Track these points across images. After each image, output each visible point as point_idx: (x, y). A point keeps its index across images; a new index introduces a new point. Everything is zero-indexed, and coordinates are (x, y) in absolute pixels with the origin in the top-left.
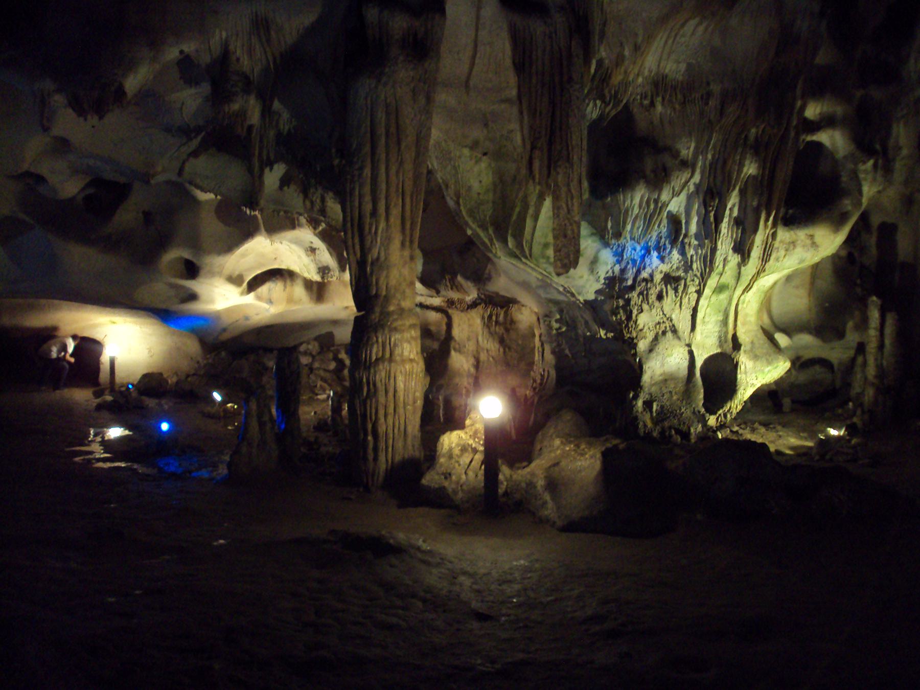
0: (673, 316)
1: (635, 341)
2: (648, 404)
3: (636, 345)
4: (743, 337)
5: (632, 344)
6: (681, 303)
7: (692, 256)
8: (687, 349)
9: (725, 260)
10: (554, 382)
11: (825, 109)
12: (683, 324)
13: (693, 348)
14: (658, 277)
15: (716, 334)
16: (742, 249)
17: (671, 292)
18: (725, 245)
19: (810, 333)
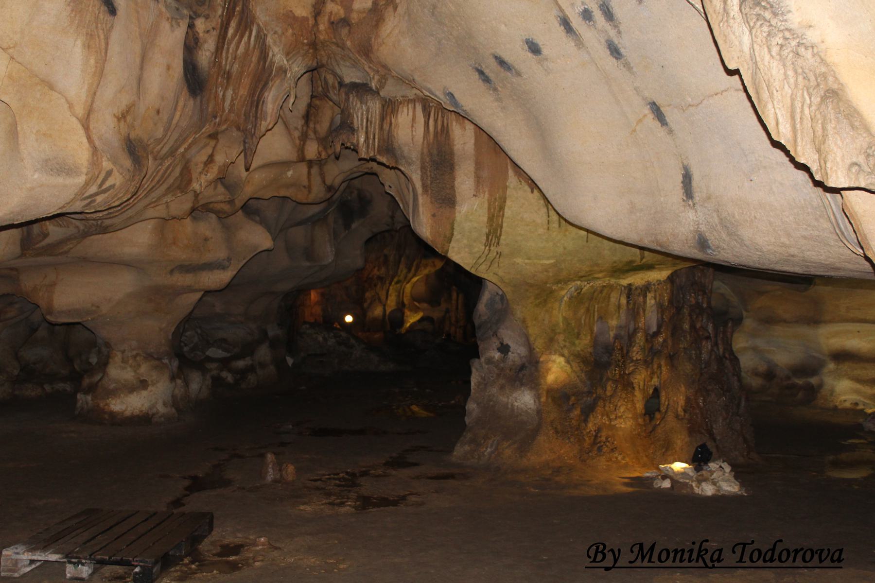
4: (406, 301)
18: (402, 266)
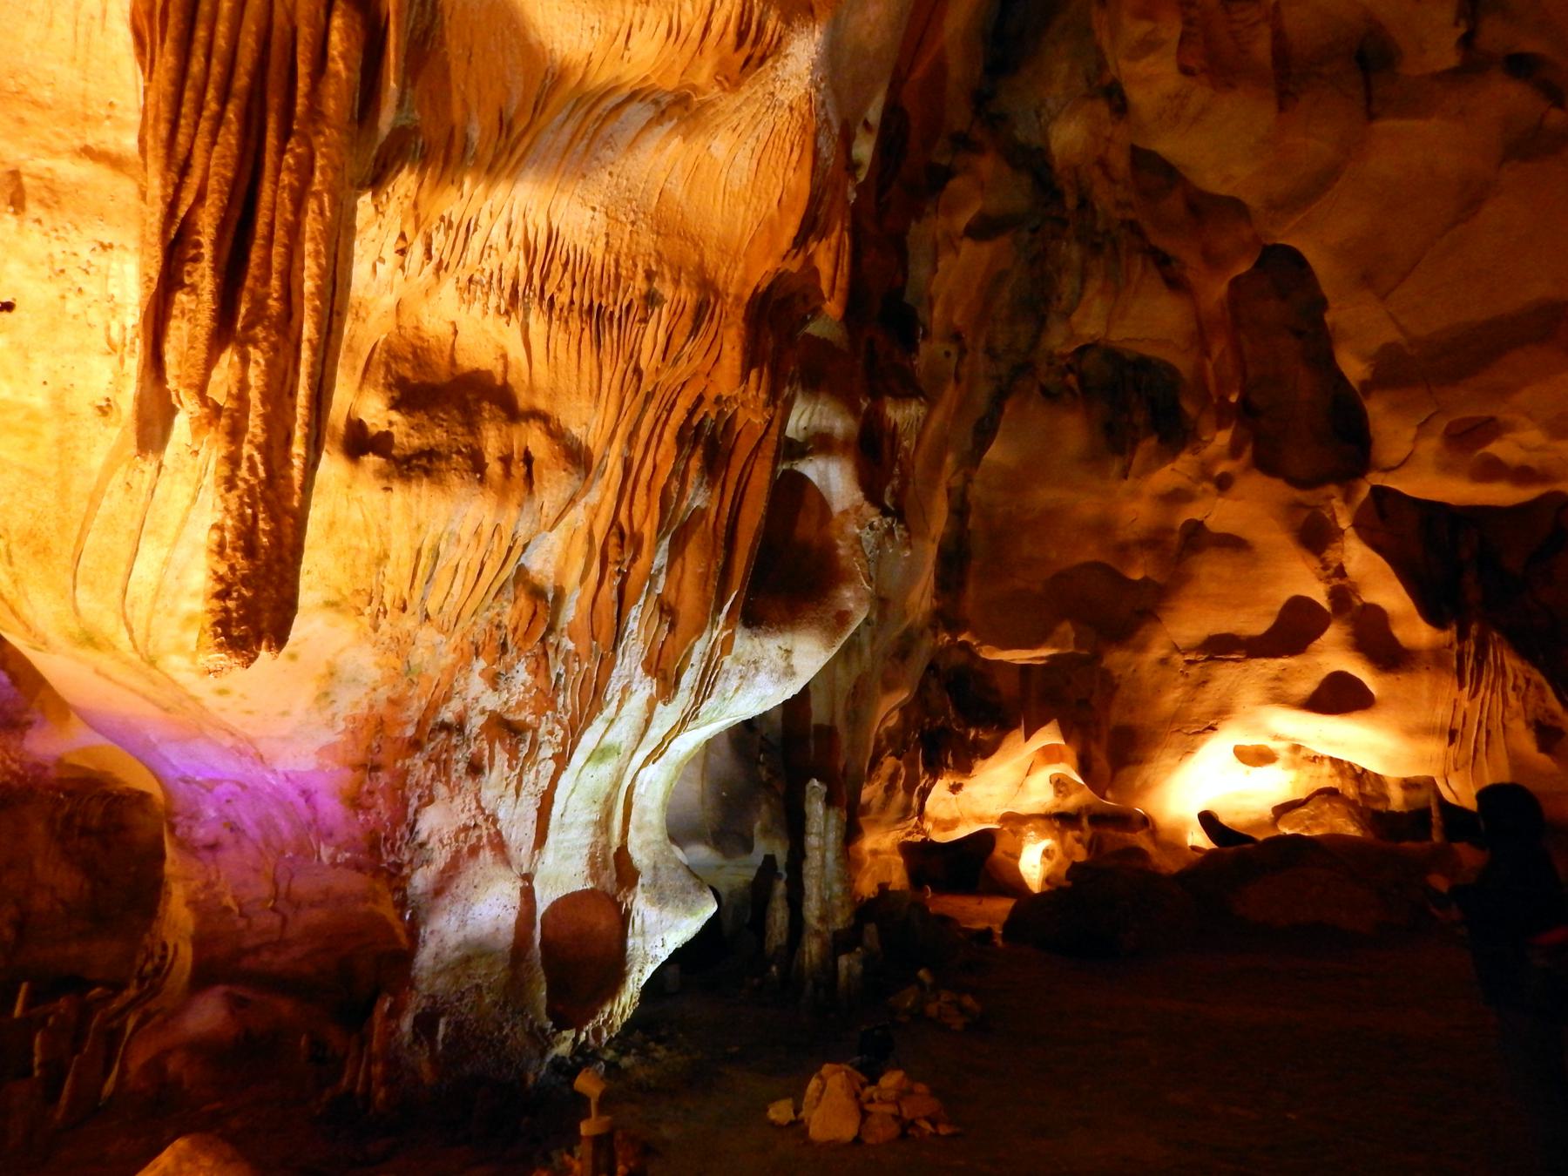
0: (501, 815)
1: (406, 871)
2: (426, 1023)
3: (408, 878)
4: (640, 855)
5: (396, 877)
6: (520, 781)
7: (559, 676)
8: (519, 884)
9: (626, 689)
10: (185, 978)
11: (816, 420)
12: (519, 832)
13: (535, 884)
14: (476, 722)
15: (586, 851)
16: (664, 672)
17: (501, 758)
19: (707, 843)
